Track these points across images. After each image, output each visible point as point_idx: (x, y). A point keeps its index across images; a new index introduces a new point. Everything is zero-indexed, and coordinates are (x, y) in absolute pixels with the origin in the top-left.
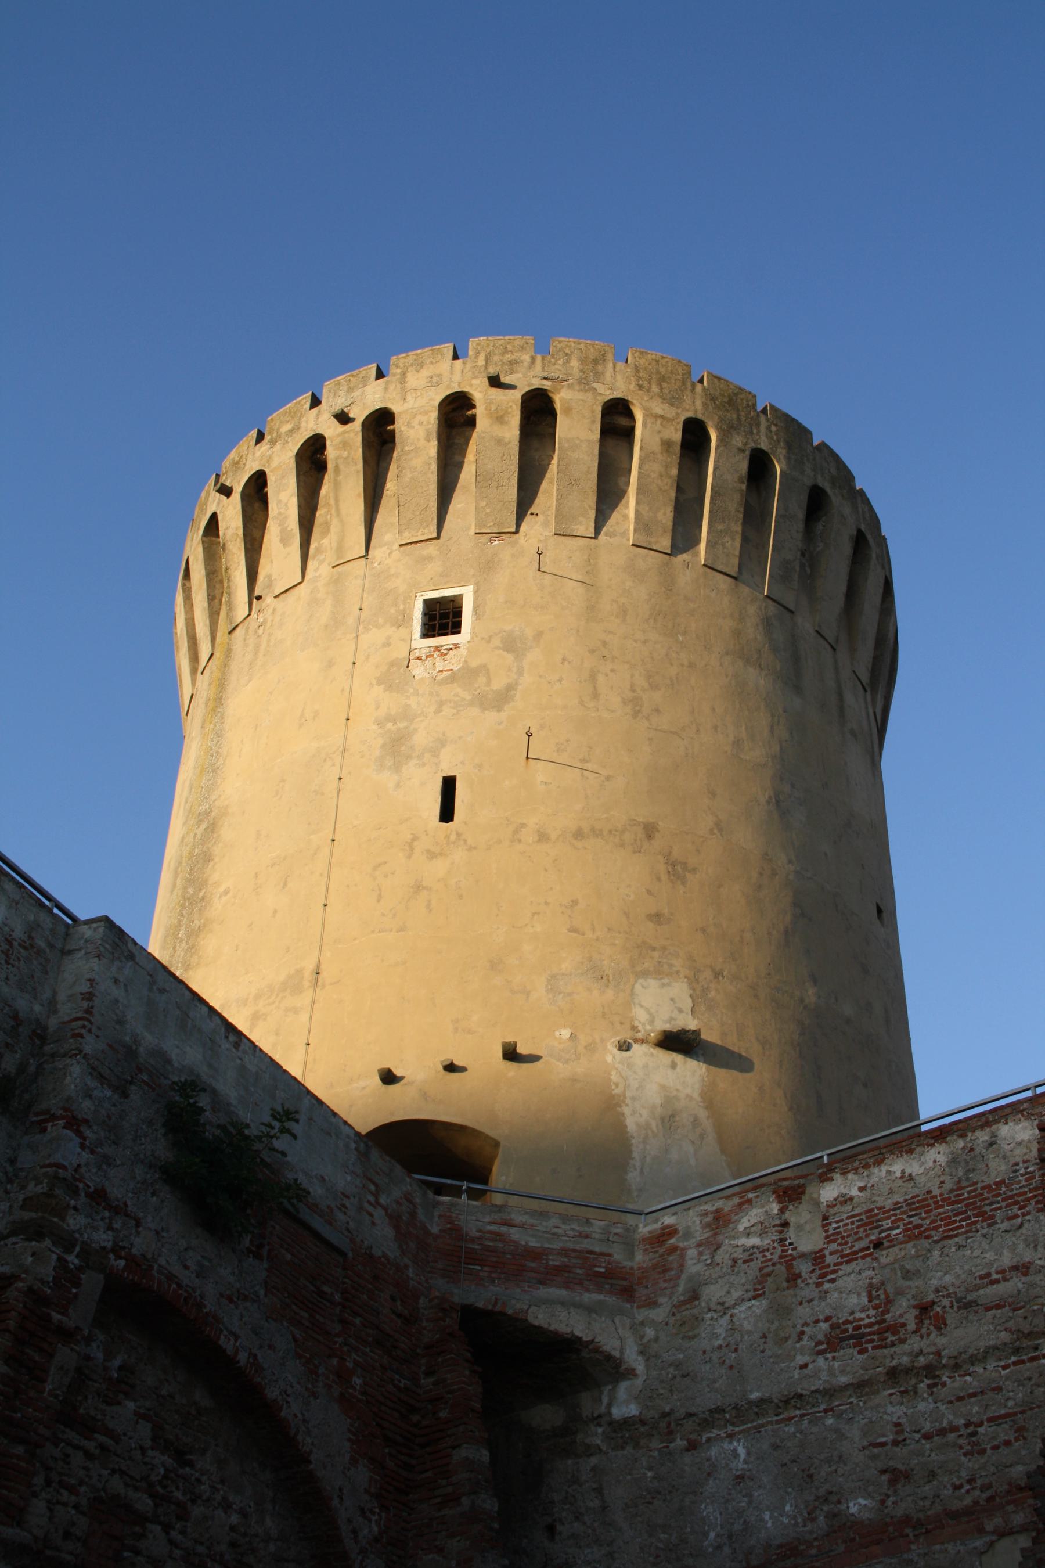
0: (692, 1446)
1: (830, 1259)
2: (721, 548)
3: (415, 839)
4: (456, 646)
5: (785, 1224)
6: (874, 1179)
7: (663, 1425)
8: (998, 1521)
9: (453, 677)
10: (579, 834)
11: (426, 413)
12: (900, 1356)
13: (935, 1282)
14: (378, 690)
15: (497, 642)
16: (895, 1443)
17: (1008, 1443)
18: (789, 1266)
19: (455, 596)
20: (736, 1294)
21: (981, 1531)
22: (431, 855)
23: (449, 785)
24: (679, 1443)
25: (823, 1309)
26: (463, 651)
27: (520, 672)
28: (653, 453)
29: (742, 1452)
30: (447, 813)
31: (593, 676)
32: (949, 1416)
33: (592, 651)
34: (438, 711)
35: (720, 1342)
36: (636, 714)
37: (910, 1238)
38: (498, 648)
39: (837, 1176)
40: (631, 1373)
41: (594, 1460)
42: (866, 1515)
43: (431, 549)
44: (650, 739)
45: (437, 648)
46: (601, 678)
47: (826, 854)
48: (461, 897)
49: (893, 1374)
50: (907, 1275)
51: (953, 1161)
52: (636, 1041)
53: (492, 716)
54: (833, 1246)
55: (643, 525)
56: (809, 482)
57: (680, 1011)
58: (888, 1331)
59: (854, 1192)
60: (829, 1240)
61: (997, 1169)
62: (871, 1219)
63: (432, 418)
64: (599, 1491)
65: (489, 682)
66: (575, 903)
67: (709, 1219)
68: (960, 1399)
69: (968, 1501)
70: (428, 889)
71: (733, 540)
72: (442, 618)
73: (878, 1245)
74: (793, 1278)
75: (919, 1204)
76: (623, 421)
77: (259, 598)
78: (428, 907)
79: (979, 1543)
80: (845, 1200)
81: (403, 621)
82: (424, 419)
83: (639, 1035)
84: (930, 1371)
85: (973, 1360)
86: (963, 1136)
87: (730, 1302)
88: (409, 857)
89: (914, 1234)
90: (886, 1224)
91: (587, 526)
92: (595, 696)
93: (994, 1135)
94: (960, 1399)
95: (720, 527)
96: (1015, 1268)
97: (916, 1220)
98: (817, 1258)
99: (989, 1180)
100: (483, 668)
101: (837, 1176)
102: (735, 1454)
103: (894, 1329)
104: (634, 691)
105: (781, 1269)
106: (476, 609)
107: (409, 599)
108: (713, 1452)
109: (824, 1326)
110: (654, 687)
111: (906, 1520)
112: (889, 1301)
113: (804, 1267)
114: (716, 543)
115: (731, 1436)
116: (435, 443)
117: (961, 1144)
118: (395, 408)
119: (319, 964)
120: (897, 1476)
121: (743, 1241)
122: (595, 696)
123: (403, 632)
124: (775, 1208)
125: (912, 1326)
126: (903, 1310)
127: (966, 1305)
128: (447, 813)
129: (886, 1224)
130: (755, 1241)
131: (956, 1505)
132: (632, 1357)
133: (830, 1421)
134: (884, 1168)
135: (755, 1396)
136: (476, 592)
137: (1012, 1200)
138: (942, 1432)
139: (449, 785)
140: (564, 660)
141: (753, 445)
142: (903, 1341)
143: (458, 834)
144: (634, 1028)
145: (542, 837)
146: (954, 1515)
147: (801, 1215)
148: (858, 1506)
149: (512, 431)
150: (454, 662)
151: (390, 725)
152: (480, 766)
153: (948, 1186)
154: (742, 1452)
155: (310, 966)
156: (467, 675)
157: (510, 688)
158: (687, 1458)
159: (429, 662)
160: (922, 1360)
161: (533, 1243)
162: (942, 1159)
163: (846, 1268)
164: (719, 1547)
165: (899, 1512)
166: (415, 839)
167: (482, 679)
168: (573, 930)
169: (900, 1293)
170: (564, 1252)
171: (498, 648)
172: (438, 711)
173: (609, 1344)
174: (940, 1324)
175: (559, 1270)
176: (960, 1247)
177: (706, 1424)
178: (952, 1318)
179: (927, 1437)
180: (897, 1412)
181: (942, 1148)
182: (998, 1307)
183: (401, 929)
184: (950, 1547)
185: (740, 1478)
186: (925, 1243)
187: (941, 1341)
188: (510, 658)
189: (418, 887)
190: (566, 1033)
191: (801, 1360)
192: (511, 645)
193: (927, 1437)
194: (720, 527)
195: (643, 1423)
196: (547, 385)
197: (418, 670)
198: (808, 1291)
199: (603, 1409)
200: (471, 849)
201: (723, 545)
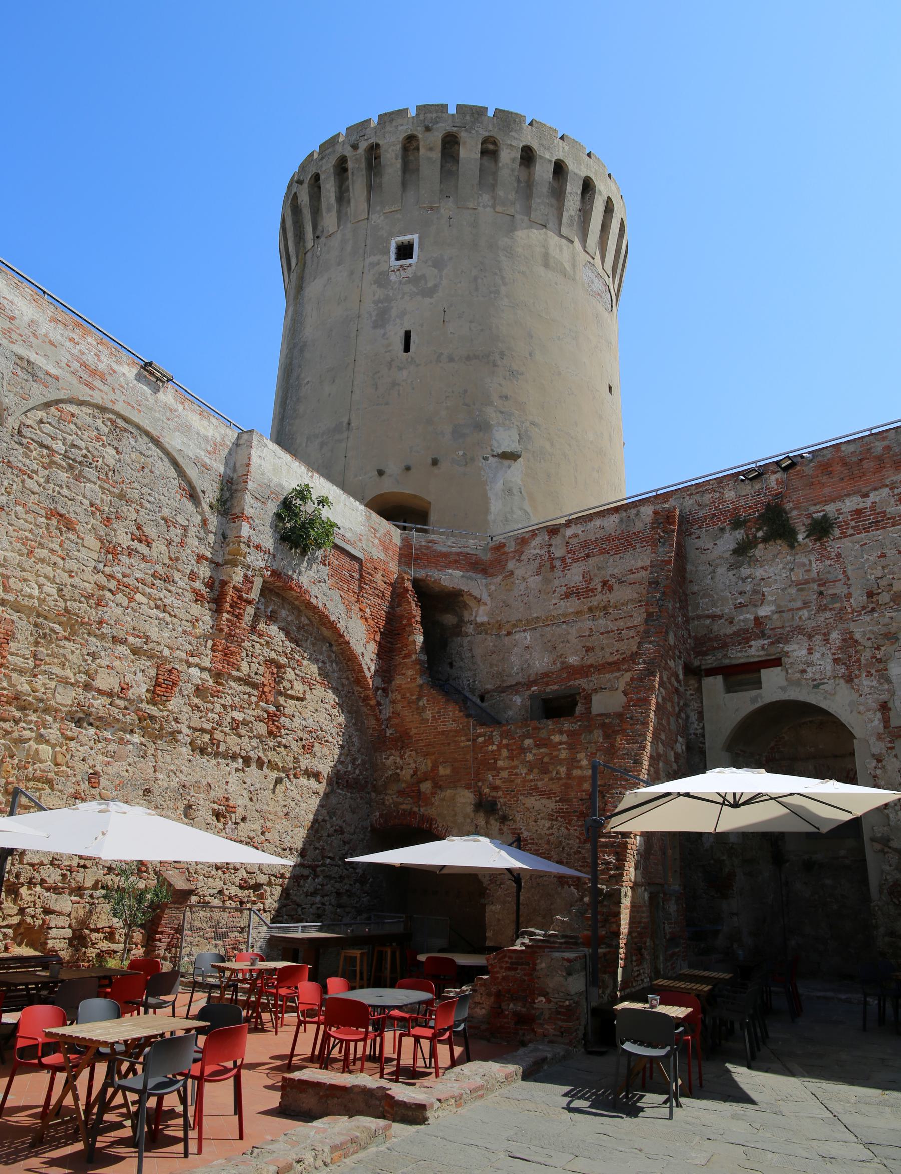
0: (509, 634)
1: (568, 561)
3: (393, 360)
4: (411, 265)
5: (550, 545)
6: (588, 527)
7: (497, 626)
8: (625, 667)
9: (410, 281)
10: (468, 358)
11: (394, 145)
12: (594, 602)
13: (610, 572)
14: (375, 287)
15: (430, 263)
16: (589, 636)
17: (633, 637)
18: (551, 563)
20: (529, 574)
21: (619, 670)
22: (400, 369)
23: (408, 335)
24: (504, 632)
25: (563, 581)
26: (414, 267)
27: (441, 278)
29: (528, 637)
30: (407, 349)
31: (475, 279)
32: (611, 626)
34: (403, 298)
35: (522, 592)
37: (601, 553)
39: (573, 525)
40: (485, 604)
41: (469, 638)
42: (576, 663)
45: (402, 266)
46: (479, 281)
48: (413, 389)
49: (590, 609)
50: (599, 568)
51: (621, 521)
52: (493, 456)
53: (428, 300)
54: (570, 555)
57: (513, 441)
58: (589, 591)
59: (580, 532)
60: (568, 552)
61: (639, 526)
62: (585, 544)
63: (399, 147)
64: (471, 650)
65: (426, 284)
66: (465, 391)
67: (519, 541)
68: (616, 620)
69: (616, 658)
70: (399, 385)
73: (588, 556)
74: (553, 567)
75: (607, 539)
77: (318, 237)
78: (399, 394)
79: (617, 674)
80: (576, 535)
83: (495, 453)
84: (605, 608)
85: (623, 605)
86: (626, 511)
87: (526, 576)
88: (390, 370)
89: (603, 551)
90: (592, 547)
92: (476, 289)
93: (638, 511)
94: (616, 620)
96: (642, 568)
97: (604, 546)
98: (563, 559)
99: (635, 531)
100: (424, 277)
101: (573, 525)
102: (526, 638)
103: (592, 590)
105: (548, 564)
107: (388, 241)
108: (517, 636)
109: (564, 588)
111: (591, 666)
112: (591, 579)
113: (557, 563)
115: (524, 631)
116: (400, 161)
117: (624, 514)
118: (381, 142)
119: (350, 419)
120: (588, 650)
121: (533, 551)
123: (385, 257)
124: (547, 537)
125: (599, 590)
126: (596, 583)
127: (621, 582)
128: (407, 349)
129: (592, 547)
130: (537, 551)
131: (611, 660)
132: (485, 597)
133: (564, 626)
134: (593, 523)
135: (535, 615)
136: (420, 238)
137: (643, 540)
138: (608, 632)
139: (408, 335)
140: (462, 272)
142: (595, 595)
143: (412, 359)
144: (492, 450)
145: (451, 360)
146: (610, 664)
147: (557, 540)
148: (573, 660)
149: (437, 155)
150: (410, 272)
151: (380, 305)
152: (422, 326)
153: (619, 532)
154: (528, 637)
155: (346, 420)
156: (415, 280)
157: (436, 286)
158: (506, 638)
159: (398, 273)
160: (602, 604)
161: (445, 549)
162: (617, 520)
163: (575, 565)
164: (518, 673)
165: (589, 662)
166: (393, 360)
167: (423, 282)
168: (466, 405)
169: (595, 575)
170: (458, 554)
172: (403, 298)
173: (476, 593)
174: (611, 589)
175: (456, 561)
176: (621, 558)
177: (515, 626)
178: (615, 587)
179: (602, 634)
180: (590, 624)
181: (615, 515)
182: (634, 583)
183: (387, 404)
184: (607, 675)
185: (527, 647)
186: (607, 556)
187: (610, 596)
188: (436, 271)
189: (394, 384)
190: (461, 453)
191: (554, 601)
192: (438, 264)
193: (602, 634)
195: (489, 624)
197: (393, 278)
198: (558, 573)
199: (473, 618)
200: (418, 366)
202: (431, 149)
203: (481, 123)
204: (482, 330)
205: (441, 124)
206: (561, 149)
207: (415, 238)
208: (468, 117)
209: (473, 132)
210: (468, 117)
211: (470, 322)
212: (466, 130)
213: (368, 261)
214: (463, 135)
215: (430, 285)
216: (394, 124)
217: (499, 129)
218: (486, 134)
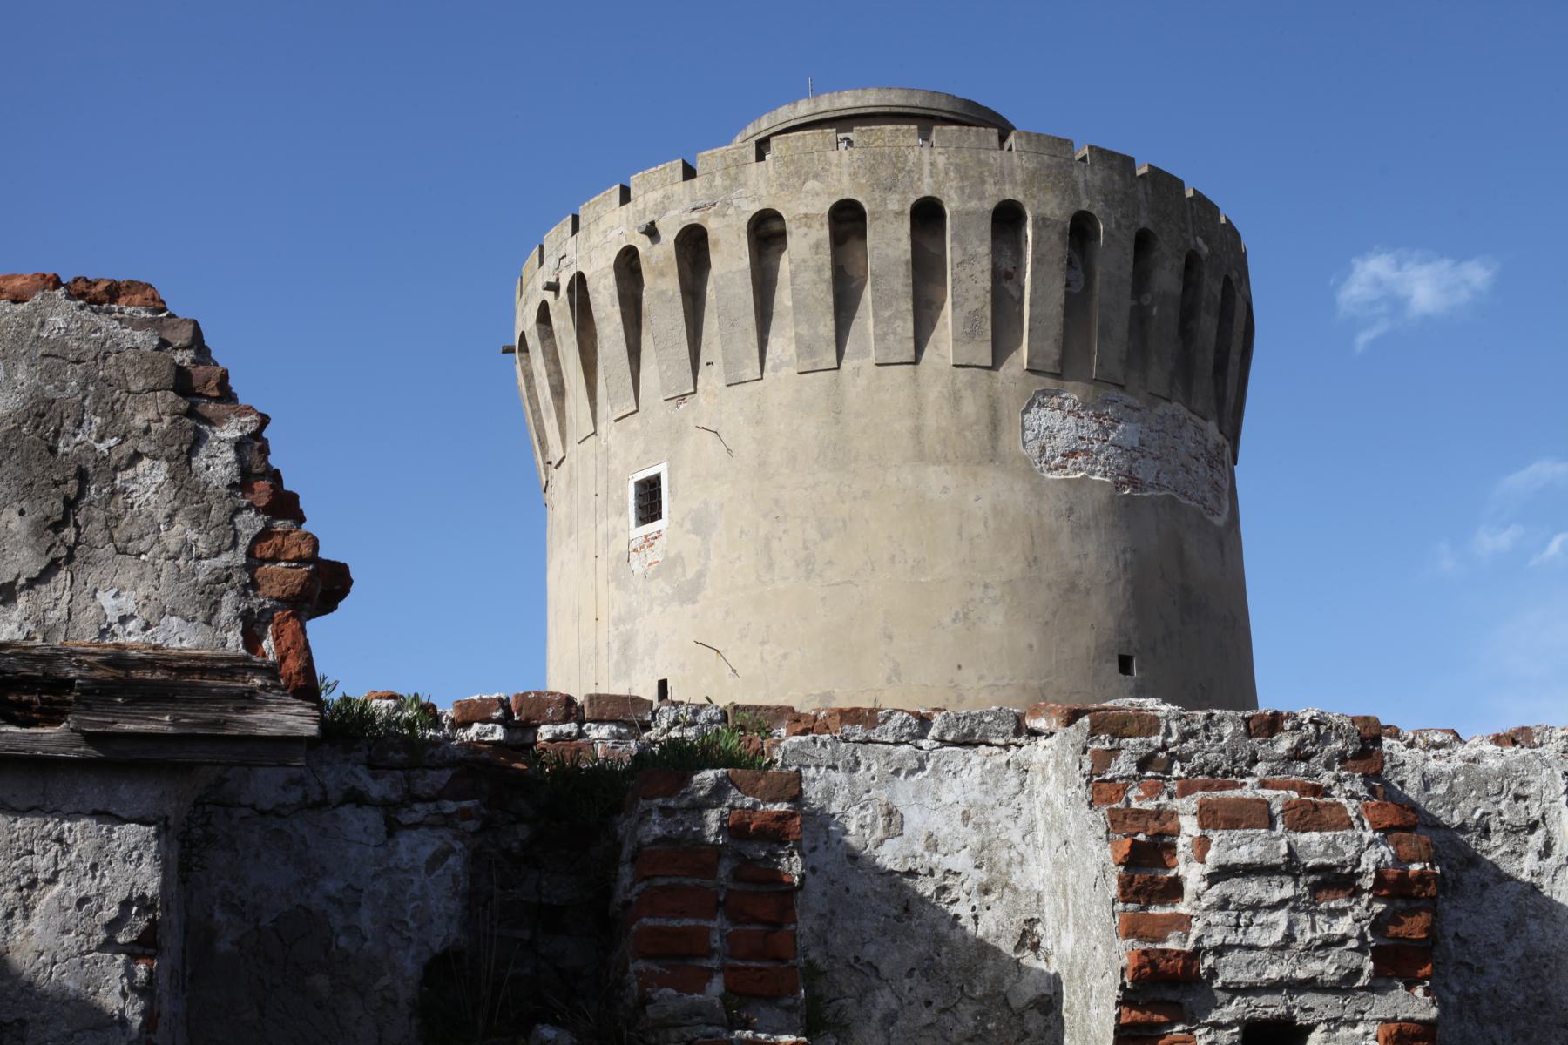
2: (891, 337)
11: (605, 276)
15: (688, 525)
19: (639, 496)
27: (708, 558)
28: (804, 261)
33: (765, 516)
34: (651, 610)
36: (809, 574)
38: (688, 532)
43: (634, 422)
44: (823, 599)
46: (775, 544)
47: (1031, 646)
55: (806, 348)
56: (989, 205)
71: (905, 321)
72: (649, 500)
76: (775, 226)
81: (622, 512)
82: (604, 281)
91: (752, 370)
92: (770, 566)
95: (887, 313)
104: (806, 548)
106: (670, 486)
110: (825, 536)
114: (886, 334)
116: (618, 308)
122: (770, 566)
136: (669, 469)
141: (913, 198)
151: (622, 628)
152: (682, 666)
156: (666, 568)
157: (700, 575)
167: (679, 569)
171: (688, 532)
188: (699, 540)
194: (887, 313)
196: (695, 218)
201: (895, 333)
202: (662, 274)
203: (744, 185)
204: (785, 656)
205: (672, 213)
206: (926, 169)
207: (662, 469)
208: (718, 181)
209: (731, 211)
210: (718, 181)
211: (763, 643)
212: (717, 214)
213: (602, 528)
214: (713, 226)
215: (691, 574)
216: (602, 227)
217: (781, 186)
218: (755, 208)
